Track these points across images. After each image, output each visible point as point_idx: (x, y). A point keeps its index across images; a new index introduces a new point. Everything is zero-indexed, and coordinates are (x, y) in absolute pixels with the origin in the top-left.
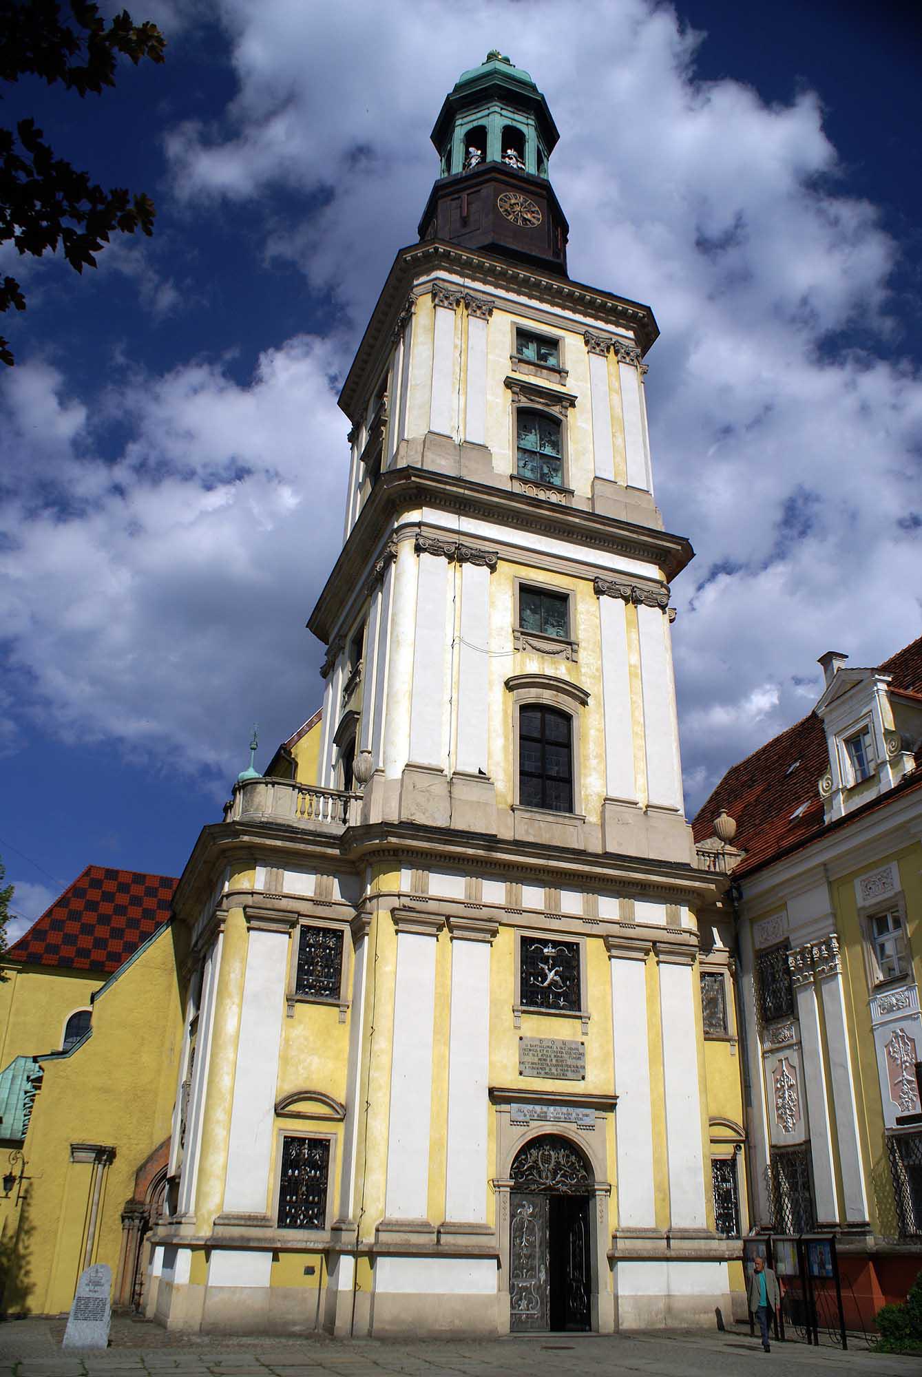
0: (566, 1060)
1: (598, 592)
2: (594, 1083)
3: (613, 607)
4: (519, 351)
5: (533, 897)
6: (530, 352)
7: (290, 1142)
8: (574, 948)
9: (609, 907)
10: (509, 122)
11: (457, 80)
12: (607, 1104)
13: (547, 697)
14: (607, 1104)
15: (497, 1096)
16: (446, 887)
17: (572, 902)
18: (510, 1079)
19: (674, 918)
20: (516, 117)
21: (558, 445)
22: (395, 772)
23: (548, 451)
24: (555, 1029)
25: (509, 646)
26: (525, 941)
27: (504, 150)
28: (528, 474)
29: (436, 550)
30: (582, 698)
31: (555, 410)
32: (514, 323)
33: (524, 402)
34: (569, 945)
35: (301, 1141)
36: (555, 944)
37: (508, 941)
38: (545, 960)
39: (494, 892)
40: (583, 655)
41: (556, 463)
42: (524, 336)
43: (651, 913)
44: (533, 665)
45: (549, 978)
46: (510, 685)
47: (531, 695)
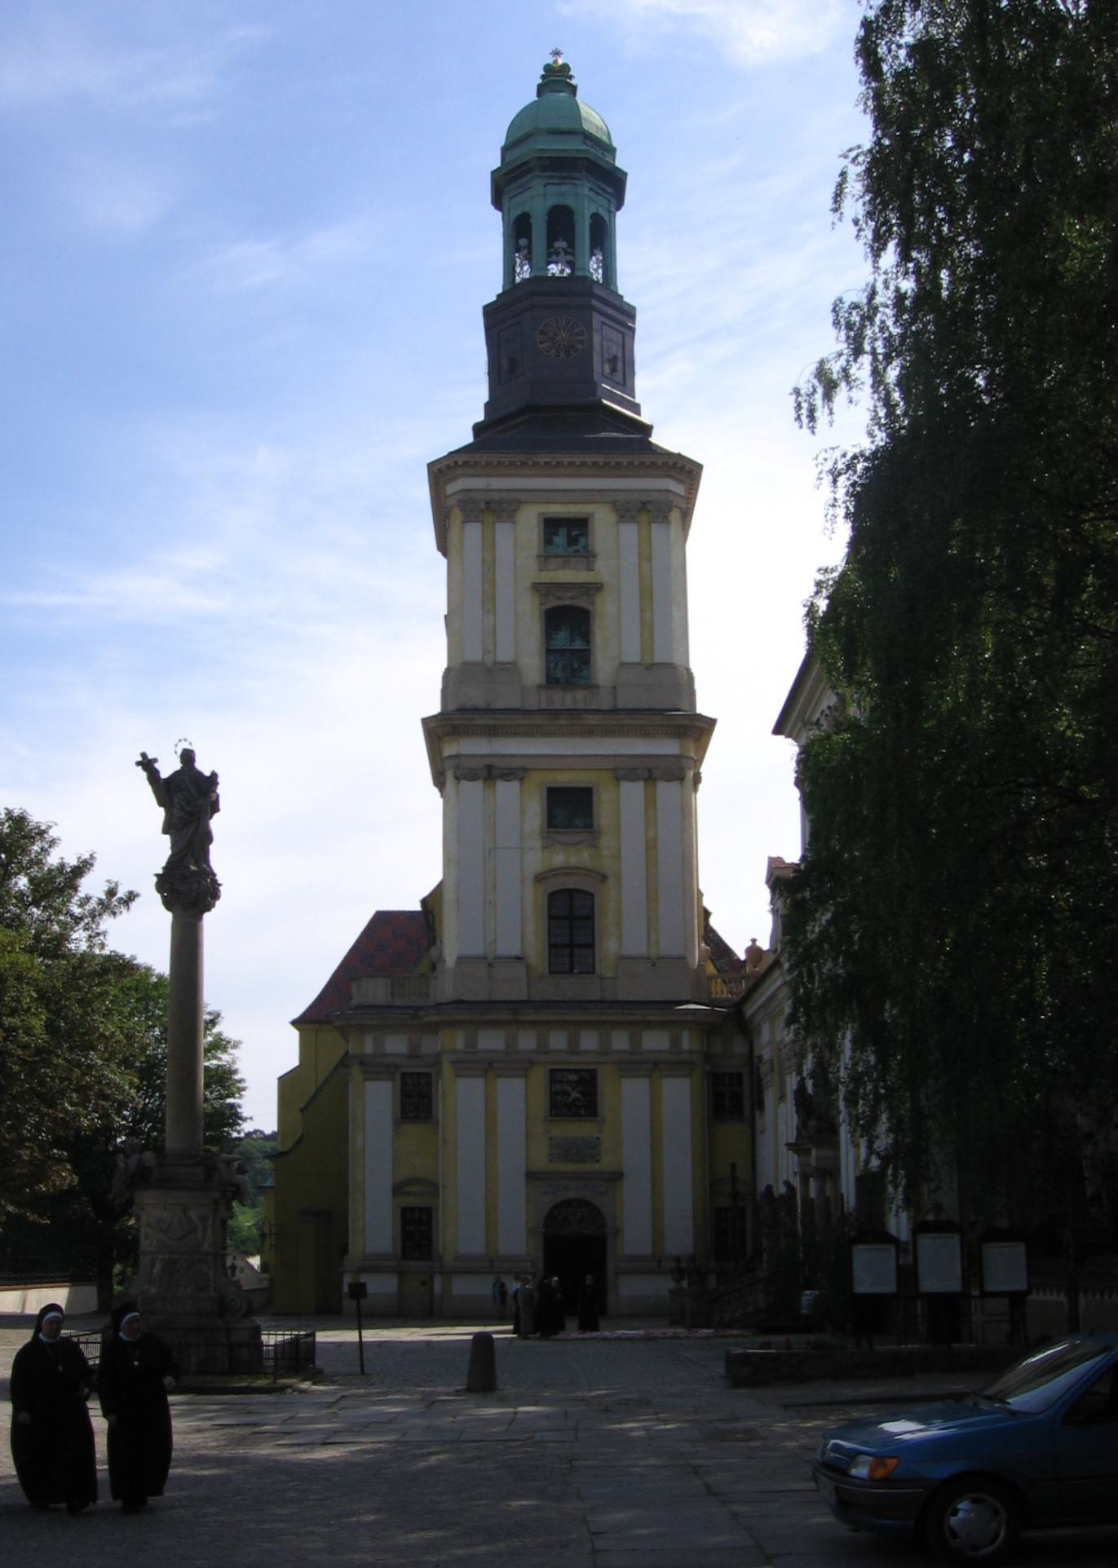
0: (588, 1150)
1: (618, 779)
2: (607, 1162)
3: (633, 791)
4: (548, 542)
5: (558, 1040)
6: (560, 539)
7: (405, 1211)
8: (593, 1074)
9: (620, 1041)
10: (552, 202)
11: (501, 141)
12: (617, 1176)
13: (571, 883)
14: (617, 1176)
15: (531, 1176)
16: (491, 1041)
17: (589, 1041)
18: (542, 1163)
19: (675, 1042)
20: (564, 188)
21: (586, 636)
22: (450, 961)
23: (578, 645)
24: (580, 1130)
25: (539, 845)
26: (552, 1071)
27: (550, 245)
28: (559, 674)
29: (470, 776)
30: (604, 878)
31: (581, 602)
32: (540, 514)
33: (553, 603)
34: (589, 1071)
35: (412, 1209)
36: (576, 1071)
37: (539, 1076)
38: (569, 1082)
39: (527, 1041)
40: (606, 842)
41: (584, 657)
42: (551, 525)
43: (656, 1041)
44: (559, 859)
45: (574, 1096)
46: (539, 879)
47: (556, 884)
